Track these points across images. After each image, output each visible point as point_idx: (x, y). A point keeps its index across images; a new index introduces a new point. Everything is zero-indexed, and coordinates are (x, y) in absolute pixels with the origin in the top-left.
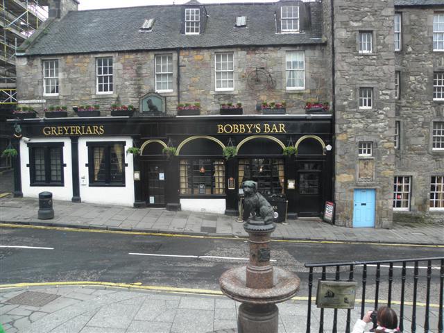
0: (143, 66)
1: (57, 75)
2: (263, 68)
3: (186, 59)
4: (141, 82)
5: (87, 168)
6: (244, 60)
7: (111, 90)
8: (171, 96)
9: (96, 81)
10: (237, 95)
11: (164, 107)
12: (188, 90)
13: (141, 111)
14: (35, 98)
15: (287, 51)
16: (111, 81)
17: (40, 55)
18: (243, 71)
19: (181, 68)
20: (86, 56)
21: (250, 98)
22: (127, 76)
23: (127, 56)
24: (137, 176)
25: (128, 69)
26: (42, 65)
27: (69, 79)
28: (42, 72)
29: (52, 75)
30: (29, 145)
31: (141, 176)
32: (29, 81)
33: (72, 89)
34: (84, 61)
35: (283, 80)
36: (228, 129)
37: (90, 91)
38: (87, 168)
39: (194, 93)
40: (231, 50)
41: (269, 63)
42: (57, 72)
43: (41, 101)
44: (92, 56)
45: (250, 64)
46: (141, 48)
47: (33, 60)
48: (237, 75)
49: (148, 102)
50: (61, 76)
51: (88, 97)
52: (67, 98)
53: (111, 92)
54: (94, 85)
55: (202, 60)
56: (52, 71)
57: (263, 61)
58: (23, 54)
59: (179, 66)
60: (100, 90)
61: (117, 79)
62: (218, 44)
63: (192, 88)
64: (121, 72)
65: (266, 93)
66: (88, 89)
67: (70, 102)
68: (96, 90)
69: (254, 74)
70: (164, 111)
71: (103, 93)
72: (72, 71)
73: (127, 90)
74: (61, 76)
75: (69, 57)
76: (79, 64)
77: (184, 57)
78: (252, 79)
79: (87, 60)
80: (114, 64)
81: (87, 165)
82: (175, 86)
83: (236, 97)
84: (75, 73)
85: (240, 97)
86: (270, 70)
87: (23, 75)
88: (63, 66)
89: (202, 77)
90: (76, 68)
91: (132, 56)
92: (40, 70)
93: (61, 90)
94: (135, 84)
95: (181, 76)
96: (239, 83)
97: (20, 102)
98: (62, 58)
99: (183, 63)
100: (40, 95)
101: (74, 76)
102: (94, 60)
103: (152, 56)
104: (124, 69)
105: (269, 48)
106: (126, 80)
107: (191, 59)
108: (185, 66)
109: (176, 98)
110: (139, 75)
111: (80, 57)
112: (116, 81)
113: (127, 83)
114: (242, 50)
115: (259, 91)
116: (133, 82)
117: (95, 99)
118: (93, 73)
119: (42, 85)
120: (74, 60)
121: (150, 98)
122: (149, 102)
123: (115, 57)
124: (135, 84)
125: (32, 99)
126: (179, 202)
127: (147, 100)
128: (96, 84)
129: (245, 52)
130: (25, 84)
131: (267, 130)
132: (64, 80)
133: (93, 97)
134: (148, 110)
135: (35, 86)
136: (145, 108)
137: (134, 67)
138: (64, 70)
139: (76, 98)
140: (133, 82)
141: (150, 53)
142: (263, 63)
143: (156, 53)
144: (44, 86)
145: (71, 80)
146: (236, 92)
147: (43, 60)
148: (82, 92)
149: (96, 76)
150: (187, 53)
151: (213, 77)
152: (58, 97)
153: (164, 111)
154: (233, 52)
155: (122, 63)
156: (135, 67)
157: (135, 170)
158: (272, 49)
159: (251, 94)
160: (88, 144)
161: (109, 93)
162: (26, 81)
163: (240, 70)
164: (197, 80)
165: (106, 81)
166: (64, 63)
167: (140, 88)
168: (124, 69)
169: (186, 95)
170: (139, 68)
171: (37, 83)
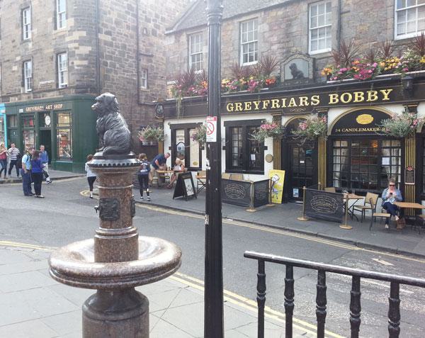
4: (291, 44)
7: (256, 60)
9: (239, 51)
11: (311, 72)
17: (186, 30)
19: (343, 15)
20: (230, 22)
22: (275, 39)
23: (273, 13)
28: (188, 48)
30: (171, 126)
44: (236, 21)
47: (179, 37)
49: (291, 68)
58: (171, 31)
64: (267, 35)
70: (311, 77)
71: (249, 64)
79: (231, 27)
80: (259, 27)
89: (375, 23)
91: (280, 13)
92: (186, 46)
94: (283, 48)
97: (168, 83)
99: (345, 9)
106: (272, 45)
108: (349, 12)
116: (282, 45)
118: (237, 42)
121: (293, 62)
122: (293, 68)
124: (283, 48)
127: (290, 65)
130: (173, 63)
134: (291, 77)
136: (289, 76)
137: (282, 27)
140: (282, 45)
147: (188, 36)
151: (390, 21)
155: (268, 24)
168: (270, 30)
170: (289, 26)
171: (183, 61)
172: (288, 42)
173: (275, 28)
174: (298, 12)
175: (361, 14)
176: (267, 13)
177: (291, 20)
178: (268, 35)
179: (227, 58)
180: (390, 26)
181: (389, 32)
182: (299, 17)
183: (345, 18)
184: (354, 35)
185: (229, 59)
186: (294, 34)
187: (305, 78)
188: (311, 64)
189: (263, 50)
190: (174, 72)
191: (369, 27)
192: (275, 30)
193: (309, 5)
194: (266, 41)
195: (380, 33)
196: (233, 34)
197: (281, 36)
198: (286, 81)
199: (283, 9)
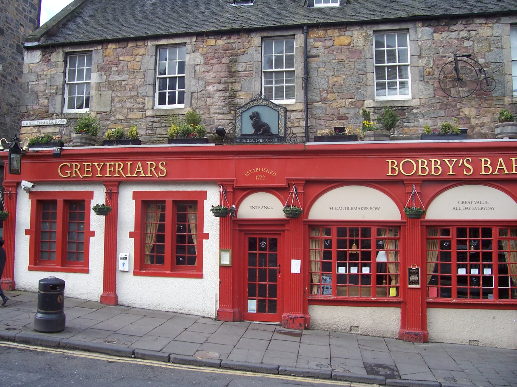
0: (241, 58)
1: (89, 77)
2: (468, 56)
3: (319, 44)
4: (237, 87)
5: (133, 239)
6: (429, 43)
8: (293, 111)
10: (417, 107)
11: (282, 127)
12: (324, 100)
13: (238, 134)
14: (50, 116)
15: (511, 24)
16: (182, 86)
18: (427, 65)
20: (140, 43)
21: (442, 113)
23: (211, 42)
24: (227, 260)
25: (213, 64)
26: (65, 61)
27: (109, 83)
28: (65, 73)
29: (80, 77)
31: (233, 258)
32: (42, 88)
33: (113, 100)
34: (135, 52)
35: (507, 77)
36: (407, 166)
37: (143, 103)
38: (133, 239)
39: (334, 105)
40: (404, 26)
41: (477, 47)
42: (89, 71)
43: (59, 122)
44: (150, 43)
45: (441, 50)
46: (237, 26)
48: (417, 70)
49: (251, 118)
50: (95, 78)
51: (138, 115)
52: (106, 115)
53: (182, 106)
54: (151, 93)
55: (349, 44)
56: (81, 72)
57: (466, 44)
58: (35, 44)
59: (307, 57)
60: (162, 101)
61: (193, 82)
62: (378, 16)
63: (330, 96)
65: (473, 103)
66: (140, 100)
67: (108, 122)
68: (154, 102)
69: (450, 67)
70: (282, 133)
71: (167, 106)
72: (114, 69)
73: (209, 101)
74: (95, 78)
75: (111, 46)
76: (127, 58)
77: (315, 41)
78: (445, 77)
79: (142, 51)
81: (131, 235)
82: (299, 92)
83: (415, 111)
84: (119, 73)
85: (424, 110)
86: (481, 61)
87: (33, 77)
88: (101, 61)
89: (351, 75)
90: (122, 64)
91: (221, 42)
92: (62, 69)
93: (92, 103)
94: (225, 90)
95: (311, 75)
96: (421, 86)
97: (24, 123)
98: (100, 47)
99: (314, 52)
100: (58, 110)
101: (118, 78)
102: (154, 49)
103: (256, 40)
104: (205, 64)
105: (478, 21)
106: (207, 84)
107: (329, 43)
108: (318, 56)
109: (302, 115)
110: (232, 74)
111: (130, 45)
112: (190, 85)
113: (210, 88)
114: (423, 26)
115: (460, 99)
116: (221, 87)
117: (153, 117)
119: (63, 94)
120: (119, 50)
121: (256, 109)
123: (191, 42)
124: (225, 90)
125: (43, 118)
126: (305, 311)
127: (250, 113)
128: (154, 92)
129: (428, 30)
131: (487, 168)
132: (99, 85)
133: (149, 113)
134: (251, 131)
135: (51, 97)
136: (248, 129)
137: (224, 60)
138: (101, 69)
139: (119, 116)
140: (221, 87)
141: (253, 35)
142: (466, 48)
143: (265, 34)
144: (66, 96)
145: (111, 86)
146: (415, 103)
147: (66, 54)
148: (129, 105)
149: (155, 78)
150: (321, 33)
151: (370, 75)
152: (88, 114)
153: (282, 133)
154: (408, 29)
156: (225, 60)
157: (223, 246)
158: (483, 21)
159: (444, 107)
160: (136, 195)
161: (177, 106)
162: (36, 89)
163: (422, 62)
164: (340, 80)
165: (172, 87)
166: (101, 56)
167: (233, 96)
169: (321, 107)
170: (234, 62)
172: (232, 83)
173: (211, 62)
174: (248, 46)
175: (334, 61)
176: (200, 39)
177: (237, 55)
178: (203, 69)
179: (134, 93)
180: (369, 83)
181: (369, 89)
182: (250, 51)
183: (314, 63)
184: (325, 87)
185: (137, 96)
186: (242, 74)
187: (272, 134)
188: (282, 114)
189: (193, 89)
190: (36, 107)
191: (344, 79)
192: (213, 64)
193: (262, 38)
194: (197, 78)
195: (358, 89)
196: (144, 61)
197: (222, 74)
198: (244, 136)
199: (225, 38)
